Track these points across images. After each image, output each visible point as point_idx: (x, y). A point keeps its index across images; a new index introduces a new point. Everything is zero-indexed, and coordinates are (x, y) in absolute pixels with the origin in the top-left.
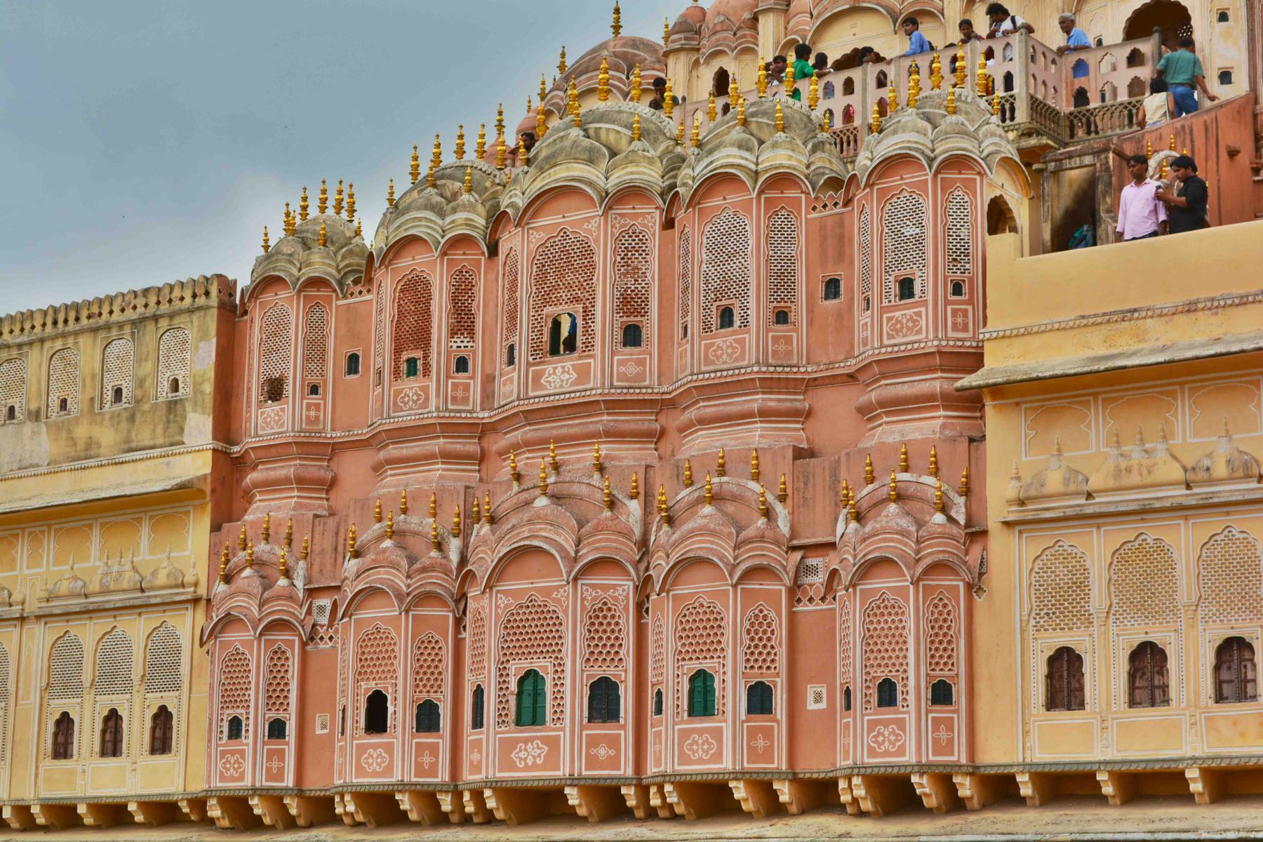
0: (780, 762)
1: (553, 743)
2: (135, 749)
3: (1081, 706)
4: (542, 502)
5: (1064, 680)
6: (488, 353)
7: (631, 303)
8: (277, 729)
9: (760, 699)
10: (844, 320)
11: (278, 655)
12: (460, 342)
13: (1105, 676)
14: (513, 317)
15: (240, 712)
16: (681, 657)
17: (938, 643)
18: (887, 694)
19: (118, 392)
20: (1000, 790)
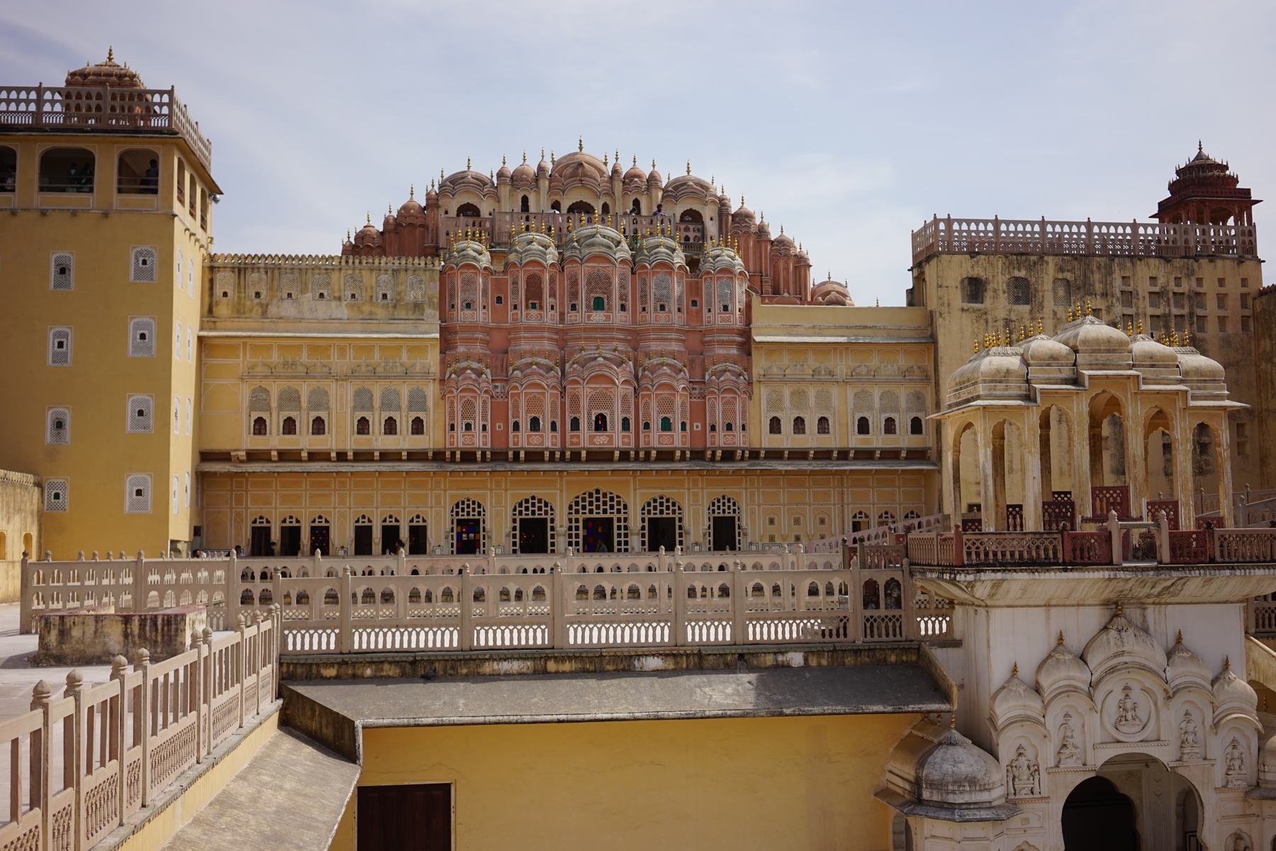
0: (688, 445)
1: (611, 437)
2: (404, 432)
3: (780, 433)
4: (601, 359)
5: (775, 425)
6: (562, 304)
7: (623, 297)
8: (484, 428)
9: (683, 428)
10: (700, 312)
11: (484, 402)
12: (552, 300)
13: (787, 426)
14: (574, 295)
15: (471, 422)
16: (659, 413)
17: (744, 412)
18: (729, 427)
19: (385, 296)
20: (754, 454)
